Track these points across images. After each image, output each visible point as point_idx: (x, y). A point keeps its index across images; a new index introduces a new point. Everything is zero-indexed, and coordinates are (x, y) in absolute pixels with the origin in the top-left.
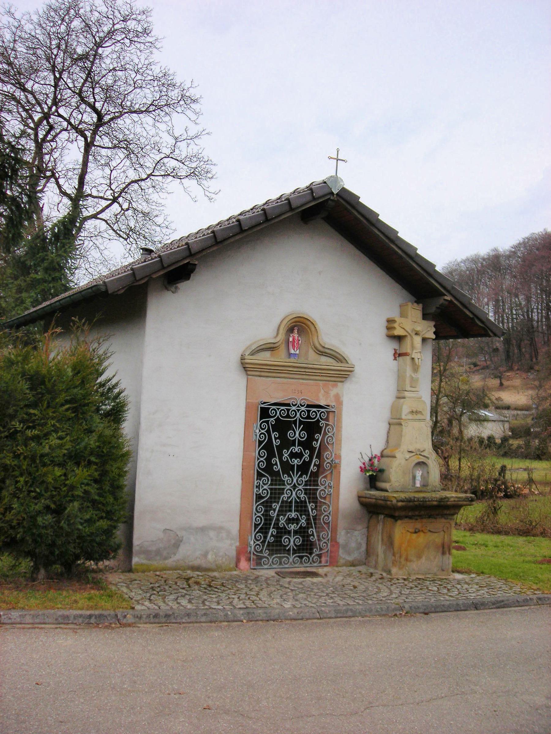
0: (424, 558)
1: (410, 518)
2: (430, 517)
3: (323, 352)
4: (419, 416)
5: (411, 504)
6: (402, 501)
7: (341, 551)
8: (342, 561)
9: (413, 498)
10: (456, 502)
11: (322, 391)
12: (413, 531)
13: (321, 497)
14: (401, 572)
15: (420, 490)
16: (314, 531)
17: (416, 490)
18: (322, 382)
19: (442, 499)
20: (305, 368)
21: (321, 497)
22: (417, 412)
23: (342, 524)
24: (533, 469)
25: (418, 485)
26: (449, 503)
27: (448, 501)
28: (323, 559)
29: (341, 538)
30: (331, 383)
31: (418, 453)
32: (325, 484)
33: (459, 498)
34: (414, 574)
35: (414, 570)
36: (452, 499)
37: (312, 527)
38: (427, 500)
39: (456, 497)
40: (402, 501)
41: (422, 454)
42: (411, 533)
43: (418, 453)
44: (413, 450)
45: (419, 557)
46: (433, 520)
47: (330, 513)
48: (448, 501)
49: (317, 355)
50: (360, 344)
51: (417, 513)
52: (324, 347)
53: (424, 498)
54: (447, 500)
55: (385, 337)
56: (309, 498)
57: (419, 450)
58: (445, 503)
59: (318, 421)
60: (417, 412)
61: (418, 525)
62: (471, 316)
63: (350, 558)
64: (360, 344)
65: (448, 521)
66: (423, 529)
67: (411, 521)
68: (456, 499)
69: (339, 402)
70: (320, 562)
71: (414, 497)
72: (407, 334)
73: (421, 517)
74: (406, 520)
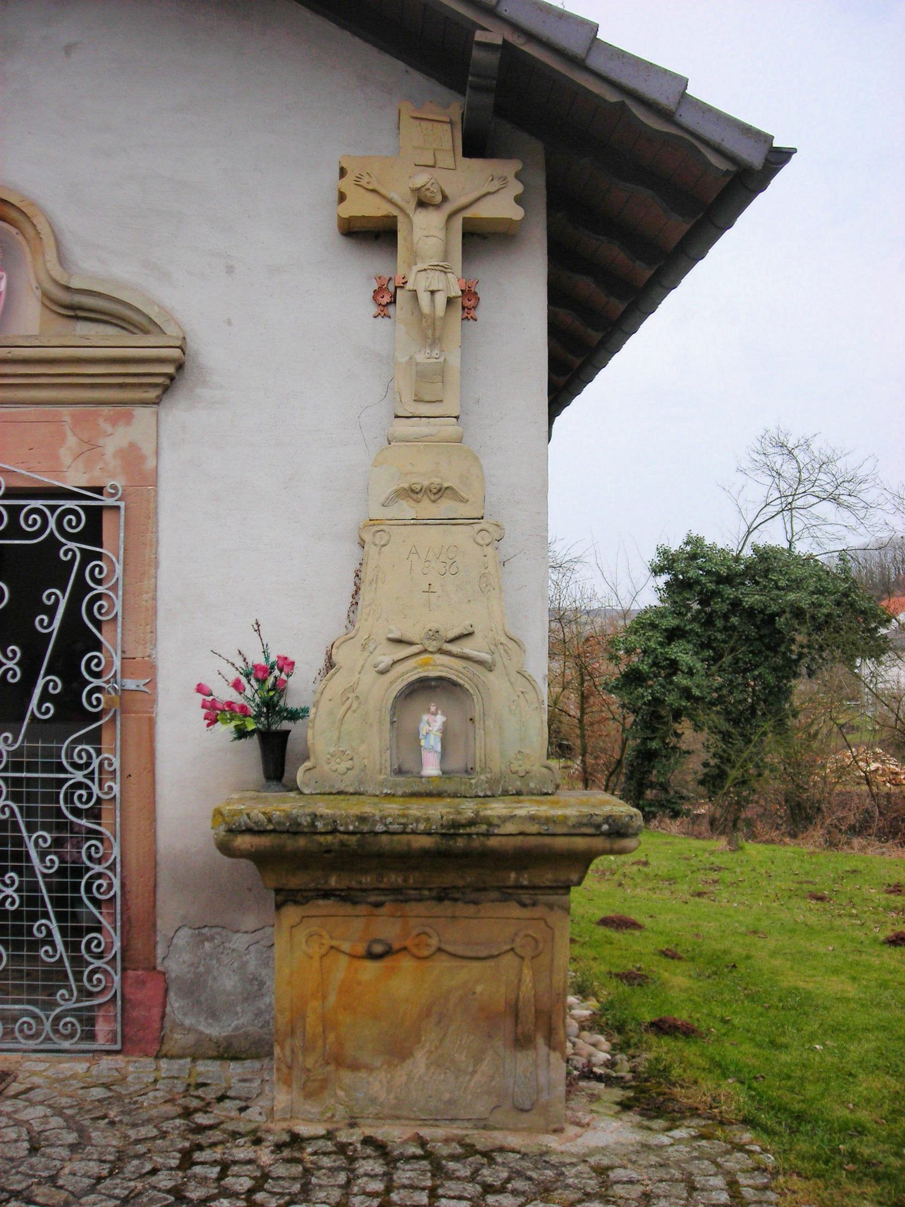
0: (420, 1058)
1: (346, 897)
2: (443, 896)
3: (76, 308)
4: (446, 507)
5: (302, 842)
6: (249, 831)
7: (175, 1003)
8: (178, 1040)
9: (305, 821)
10: (532, 841)
11: (72, 440)
12: (361, 949)
13: (76, 812)
14: (312, 1108)
15: (431, 787)
16: (54, 926)
17: (421, 789)
18: (72, 409)
19: (455, 825)
20: (141, 385)
21: (76, 812)
22: (440, 492)
23: (171, 910)
24: (624, 685)
25: (431, 768)
26: (493, 842)
27: (487, 835)
28: (101, 1028)
29: (176, 958)
30: (106, 410)
31: (432, 646)
32: (88, 765)
33: (548, 820)
34: (377, 1117)
35: (373, 1101)
36: (510, 828)
37: (46, 915)
38: (380, 828)
39: (532, 818)
40: (249, 831)
41: (454, 648)
42: (353, 956)
43: (432, 646)
44: (409, 636)
45: (398, 1051)
46: (461, 909)
47: (112, 868)
48: (487, 835)
49: (65, 321)
50: (230, 270)
51: (367, 880)
52: (68, 288)
53: (362, 819)
54: (483, 828)
55: (340, 240)
56: (28, 813)
57: (435, 634)
58: (476, 843)
59: (52, 544)
60: (440, 492)
61: (388, 928)
62: (612, 97)
63: (215, 1031)
64: (230, 270)
65: (537, 912)
66: (408, 943)
67: (348, 909)
68: (534, 828)
69: (144, 479)
70: (90, 1036)
71: (315, 816)
72: (394, 212)
73: (399, 895)
74: (324, 906)
